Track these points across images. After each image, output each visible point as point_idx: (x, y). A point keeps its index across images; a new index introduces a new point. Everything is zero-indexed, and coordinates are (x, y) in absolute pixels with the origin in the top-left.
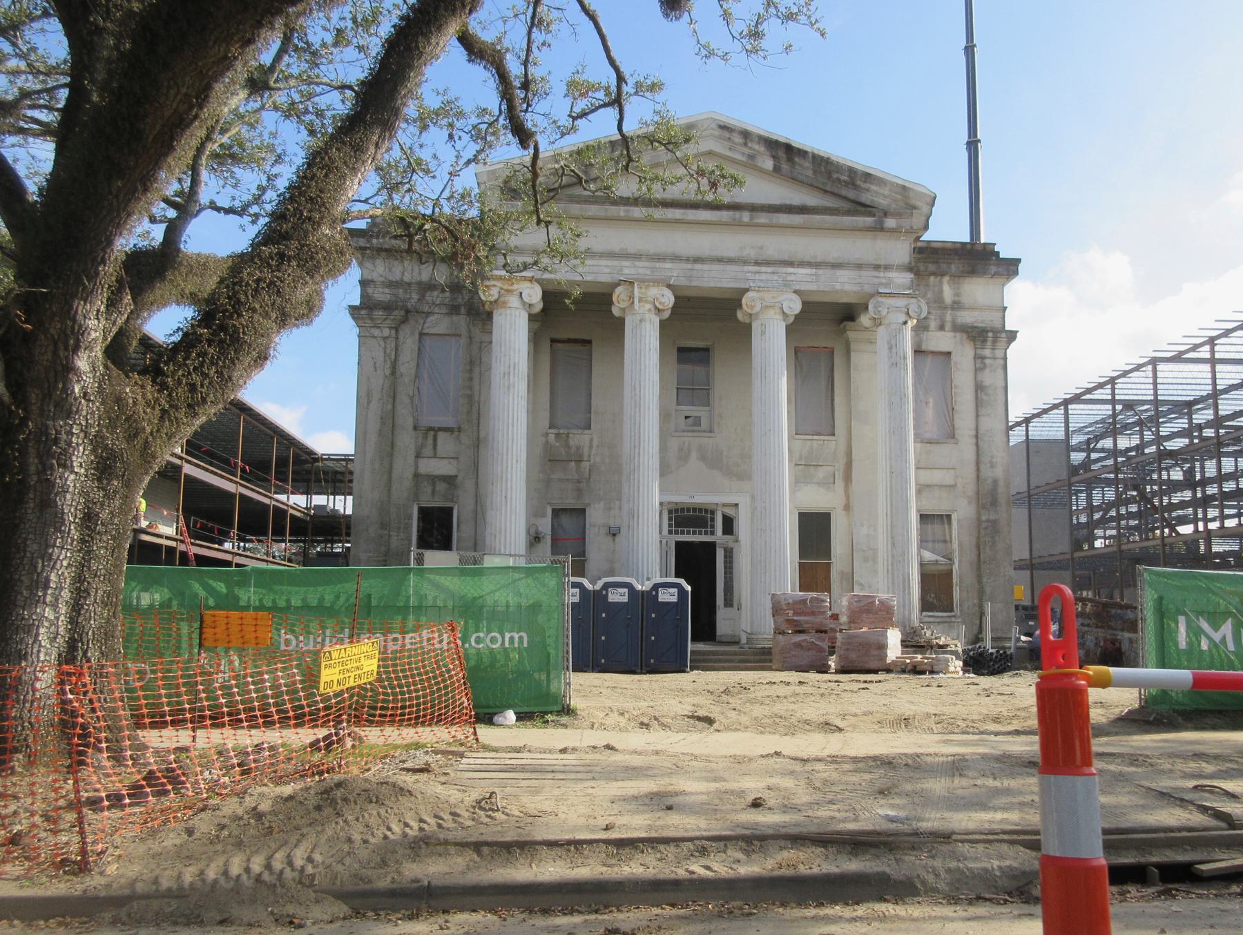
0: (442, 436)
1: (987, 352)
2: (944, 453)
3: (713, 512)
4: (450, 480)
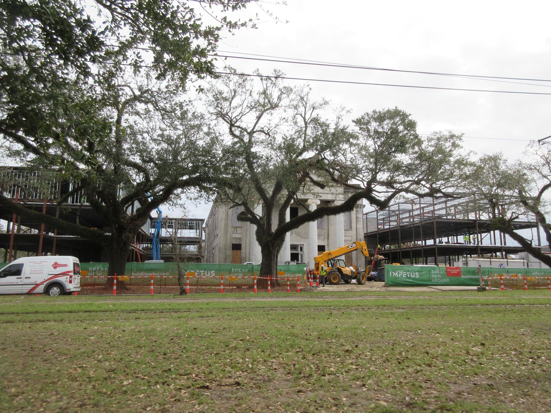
0: (238, 229)
1: (359, 210)
2: (349, 233)
4: (240, 239)
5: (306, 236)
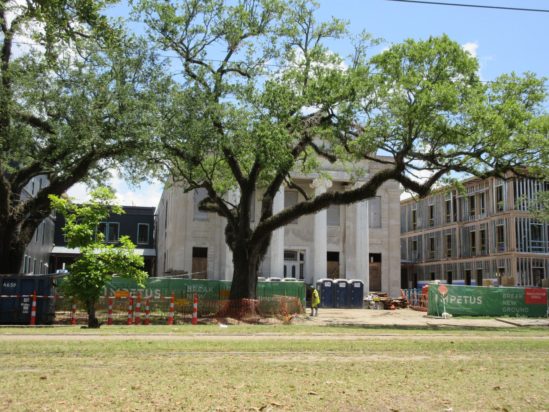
3: (296, 252)
5: (309, 237)
